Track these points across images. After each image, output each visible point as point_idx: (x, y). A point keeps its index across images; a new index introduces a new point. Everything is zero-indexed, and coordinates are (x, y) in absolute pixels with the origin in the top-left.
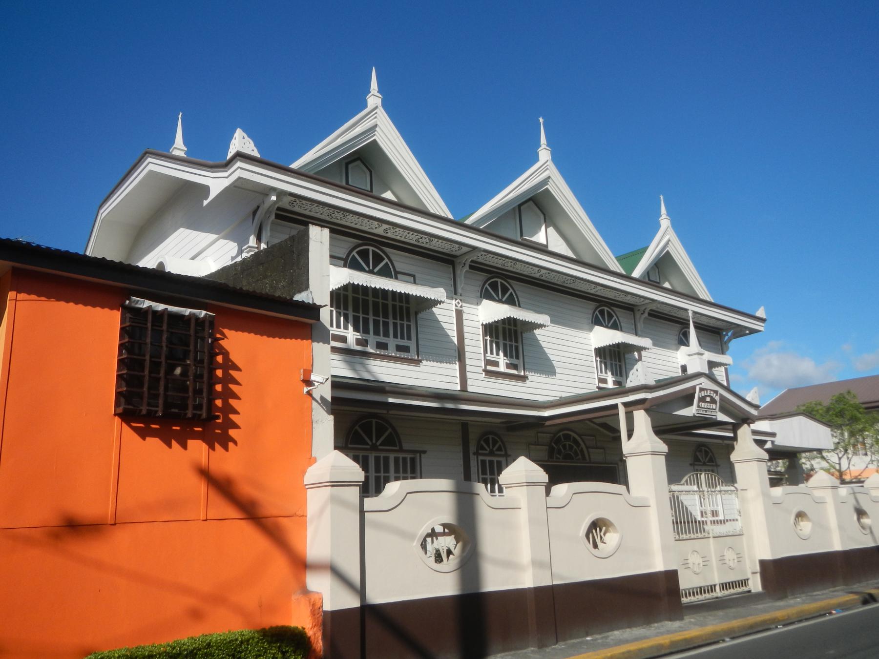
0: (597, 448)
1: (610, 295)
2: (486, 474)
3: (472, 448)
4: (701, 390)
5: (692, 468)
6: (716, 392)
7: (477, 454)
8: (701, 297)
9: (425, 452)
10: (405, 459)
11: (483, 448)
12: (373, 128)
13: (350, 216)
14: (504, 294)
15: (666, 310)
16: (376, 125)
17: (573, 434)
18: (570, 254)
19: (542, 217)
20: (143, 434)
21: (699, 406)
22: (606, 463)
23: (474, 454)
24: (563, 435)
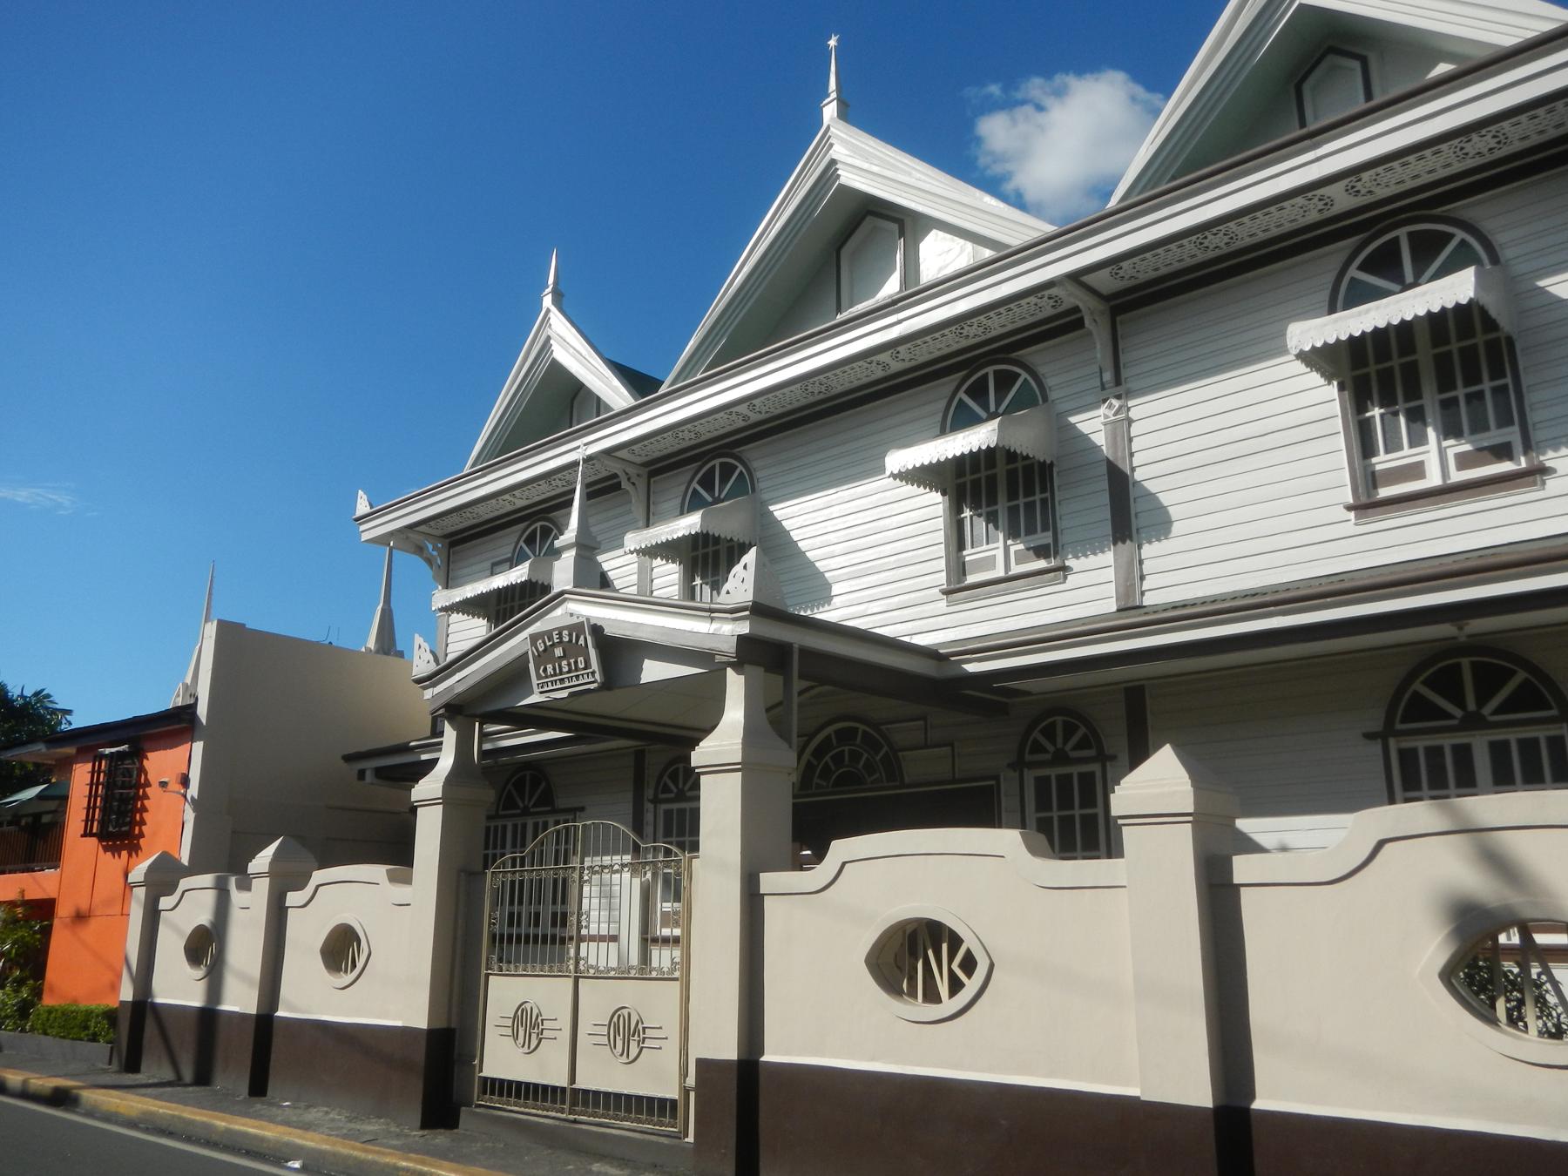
0: (926, 746)
1: (974, 334)
2: (1050, 809)
3: (649, 793)
4: (534, 638)
5: (1376, 748)
6: (577, 629)
7: (656, 801)
8: (1509, 40)
9: (582, 809)
10: (1065, 781)
11: (666, 790)
12: (547, 344)
13: (476, 509)
14: (724, 481)
15: (1191, 253)
16: (549, 338)
17: (862, 727)
18: (988, 254)
19: (895, 227)
20: (106, 849)
21: (539, 677)
22: (954, 781)
23: (651, 801)
24: (837, 732)
